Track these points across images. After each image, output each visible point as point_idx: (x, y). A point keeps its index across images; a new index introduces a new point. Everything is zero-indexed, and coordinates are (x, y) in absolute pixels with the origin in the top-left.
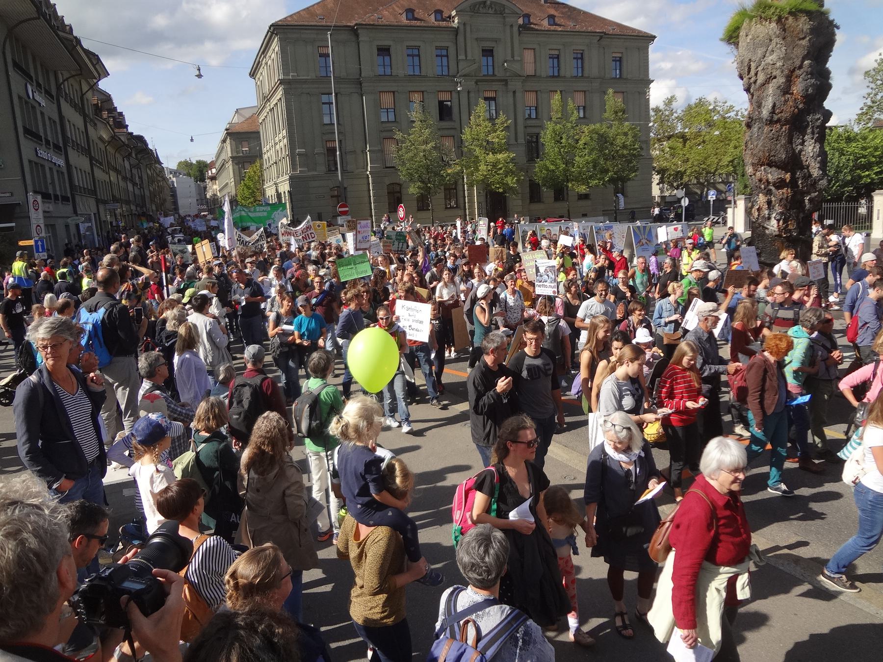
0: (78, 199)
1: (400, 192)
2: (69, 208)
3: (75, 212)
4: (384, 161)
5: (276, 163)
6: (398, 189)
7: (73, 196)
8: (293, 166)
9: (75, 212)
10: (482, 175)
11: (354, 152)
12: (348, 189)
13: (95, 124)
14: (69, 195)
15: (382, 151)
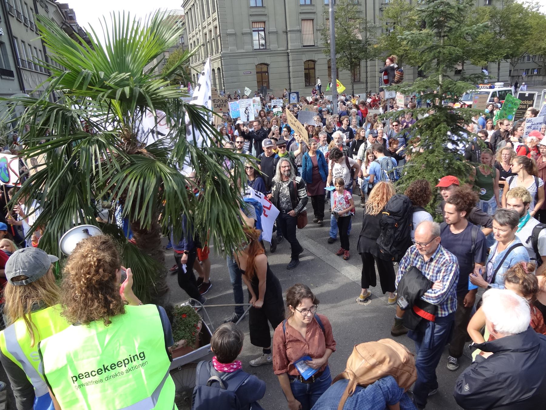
0: (26, 75)
1: (314, 68)
2: (14, 84)
3: (22, 88)
4: (301, 40)
5: (203, 45)
6: (313, 66)
7: (18, 70)
8: (225, 45)
9: (22, 88)
10: (405, 50)
11: (276, 33)
12: (270, 66)
13: (47, 7)
14: (13, 69)
15: (300, 31)
